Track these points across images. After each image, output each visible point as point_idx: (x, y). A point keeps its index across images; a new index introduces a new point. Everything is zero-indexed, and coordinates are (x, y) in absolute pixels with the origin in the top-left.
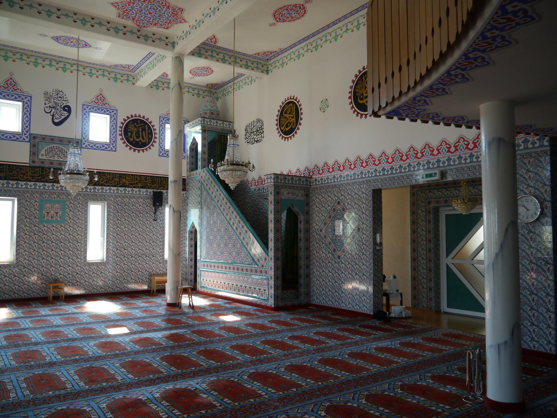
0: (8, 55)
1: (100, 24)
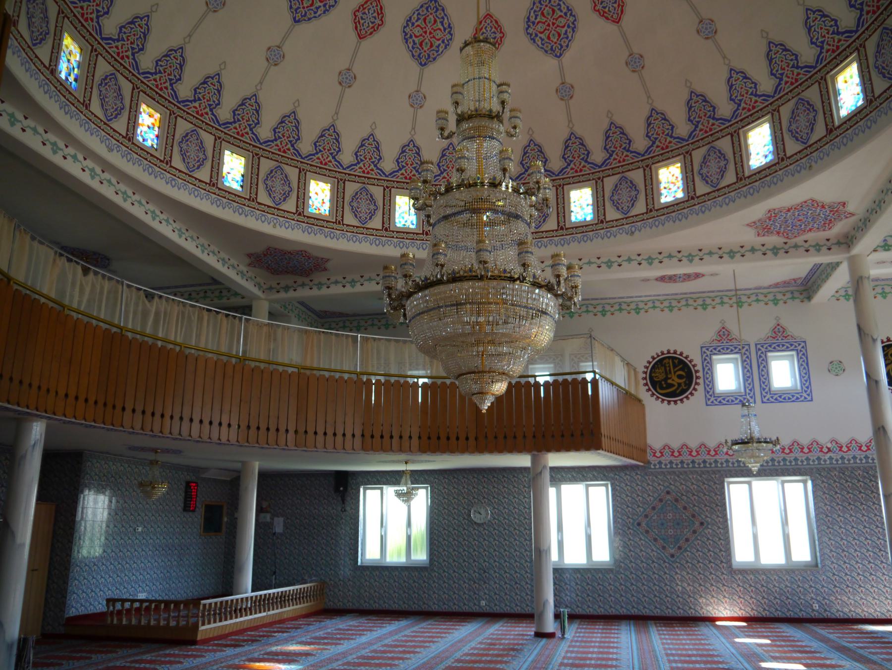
0: (707, 303)
1: (710, 253)
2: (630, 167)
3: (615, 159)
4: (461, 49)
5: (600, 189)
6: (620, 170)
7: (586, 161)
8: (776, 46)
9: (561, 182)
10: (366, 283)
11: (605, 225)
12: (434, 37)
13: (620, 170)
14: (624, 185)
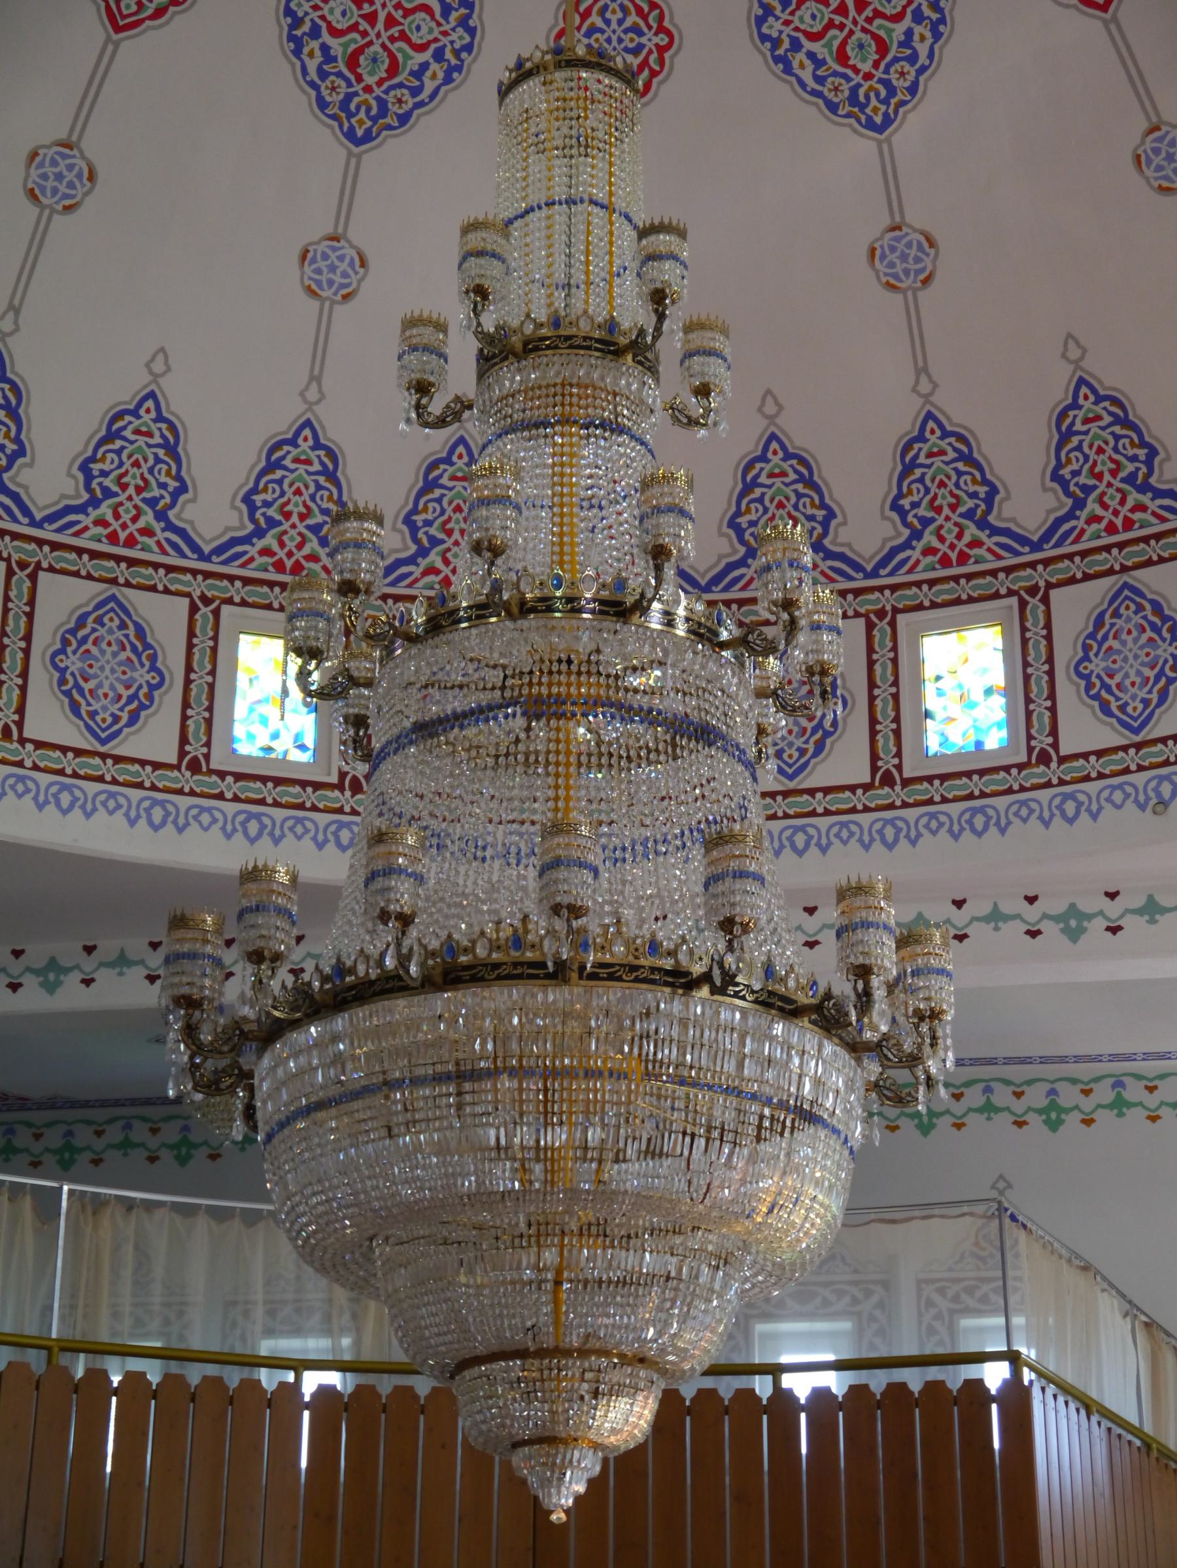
2: (1154, 550)
3: (1094, 519)
4: (504, 91)
5: (1036, 632)
6: (1115, 559)
7: (983, 524)
8: (1099, 399)
9: (887, 600)
10: (104, 977)
11: (1054, 771)
12: (403, 37)
13: (1115, 559)
14: (1130, 618)
